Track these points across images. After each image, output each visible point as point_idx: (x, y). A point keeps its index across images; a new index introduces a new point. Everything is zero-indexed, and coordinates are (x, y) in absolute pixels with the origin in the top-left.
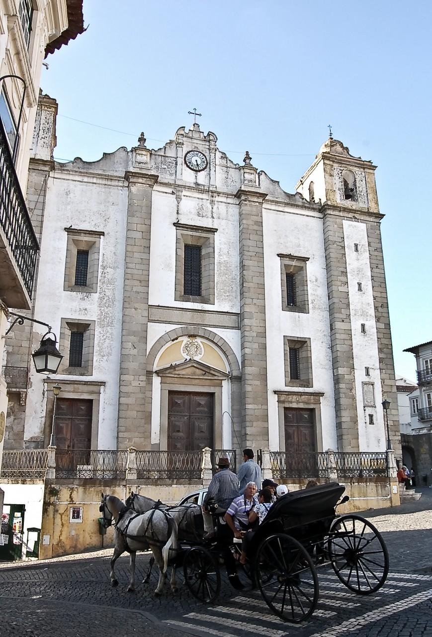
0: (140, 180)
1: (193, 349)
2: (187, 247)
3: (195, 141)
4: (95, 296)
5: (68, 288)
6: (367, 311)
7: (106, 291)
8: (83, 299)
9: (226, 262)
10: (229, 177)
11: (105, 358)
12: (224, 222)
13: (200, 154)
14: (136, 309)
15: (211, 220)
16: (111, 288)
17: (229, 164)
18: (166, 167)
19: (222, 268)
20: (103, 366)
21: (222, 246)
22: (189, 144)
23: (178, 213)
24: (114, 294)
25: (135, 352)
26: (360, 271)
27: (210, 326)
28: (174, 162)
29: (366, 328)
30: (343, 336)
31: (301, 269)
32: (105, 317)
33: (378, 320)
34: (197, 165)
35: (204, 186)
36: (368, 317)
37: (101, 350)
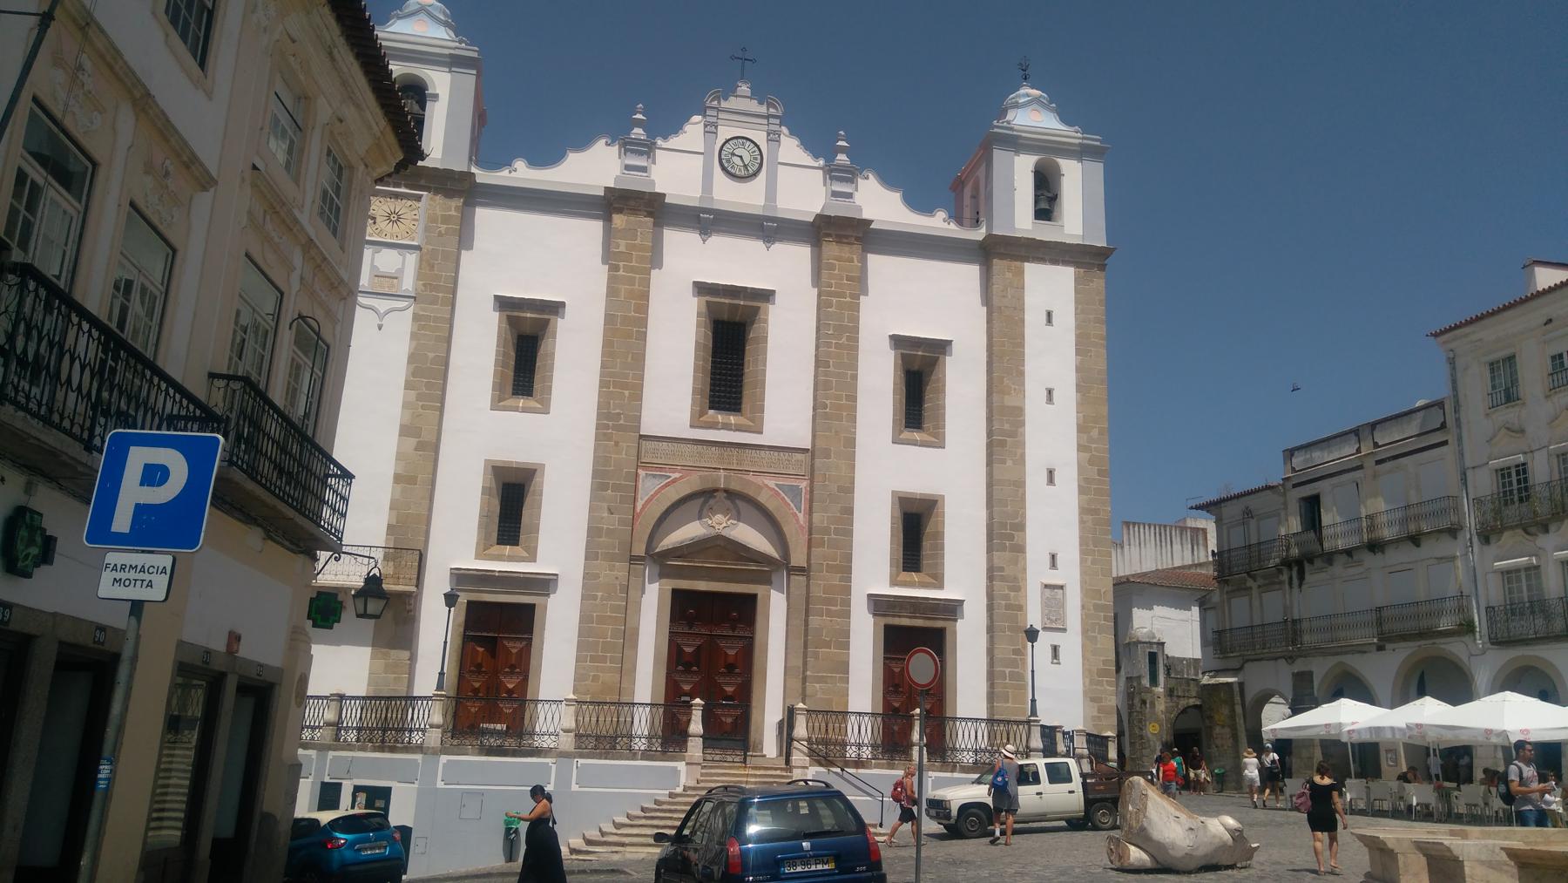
5: (498, 403)
20: (560, 543)
34: (745, 166)
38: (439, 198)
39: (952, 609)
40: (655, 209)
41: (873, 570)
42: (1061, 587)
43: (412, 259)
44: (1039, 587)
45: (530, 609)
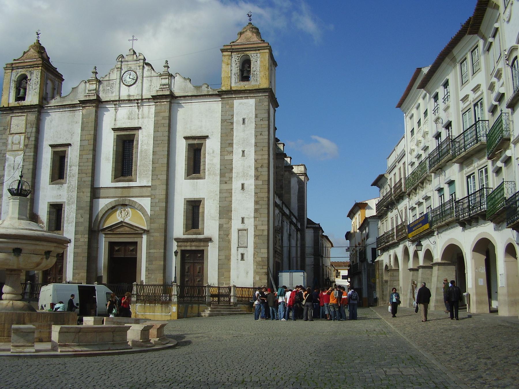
1: (123, 213)
2: (124, 142)
3: (129, 63)
4: (65, 186)
8: (59, 189)
10: (152, 84)
14: (83, 192)
15: (137, 120)
23: (115, 120)
25: (81, 220)
27: (133, 197)
29: (245, 186)
30: (225, 195)
31: (201, 144)
32: (71, 199)
33: (257, 178)
35: (133, 96)
37: (68, 220)
38: (30, 115)
39: (209, 240)
41: (178, 229)
43: (23, 137)
44: (237, 231)
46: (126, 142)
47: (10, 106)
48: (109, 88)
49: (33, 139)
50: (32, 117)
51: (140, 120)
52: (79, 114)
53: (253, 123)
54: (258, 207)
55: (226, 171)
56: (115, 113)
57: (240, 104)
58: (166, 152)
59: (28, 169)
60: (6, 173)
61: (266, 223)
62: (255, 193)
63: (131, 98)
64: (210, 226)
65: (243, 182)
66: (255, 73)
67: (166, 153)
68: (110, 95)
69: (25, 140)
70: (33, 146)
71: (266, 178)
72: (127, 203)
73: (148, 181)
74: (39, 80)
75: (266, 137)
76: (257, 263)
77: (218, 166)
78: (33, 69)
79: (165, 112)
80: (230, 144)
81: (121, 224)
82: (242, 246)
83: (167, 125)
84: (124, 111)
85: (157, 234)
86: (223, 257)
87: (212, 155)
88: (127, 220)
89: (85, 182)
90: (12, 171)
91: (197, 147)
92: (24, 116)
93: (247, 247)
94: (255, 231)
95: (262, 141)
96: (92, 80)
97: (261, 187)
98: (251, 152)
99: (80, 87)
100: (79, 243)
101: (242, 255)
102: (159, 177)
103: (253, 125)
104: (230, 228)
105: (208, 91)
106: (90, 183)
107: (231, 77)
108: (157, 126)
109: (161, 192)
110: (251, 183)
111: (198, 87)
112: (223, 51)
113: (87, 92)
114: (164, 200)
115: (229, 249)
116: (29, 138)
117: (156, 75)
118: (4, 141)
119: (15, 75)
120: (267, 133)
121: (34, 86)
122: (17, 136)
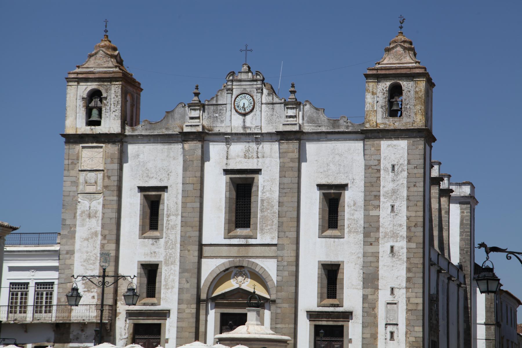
0: (192, 137)
4: (162, 241)
6: (398, 232)
7: (170, 235)
8: (153, 244)
9: (268, 199)
10: (275, 113)
11: (170, 290)
12: (268, 161)
13: (247, 96)
15: (255, 160)
16: (173, 232)
17: (276, 100)
18: (217, 115)
19: (264, 204)
21: (266, 184)
22: (238, 87)
23: (227, 158)
24: (176, 238)
26: (394, 192)
28: (225, 109)
29: (395, 249)
30: (370, 259)
33: (409, 239)
35: (250, 128)
36: (398, 238)
37: (166, 285)
38: (110, 146)
40: (203, 137)
41: (309, 297)
42: (396, 304)
45: (159, 325)
46: (242, 187)
47: (79, 132)
48: (217, 115)
49: (116, 178)
50: (113, 149)
51: (260, 160)
52: (177, 148)
53: (404, 171)
54: (410, 275)
55: (371, 231)
56: (226, 149)
57: (388, 146)
58: (296, 204)
59: (111, 219)
60: (78, 223)
61: (421, 295)
62: (408, 258)
63: (248, 131)
64: (351, 297)
65: (392, 244)
66: (408, 106)
67: (296, 204)
68: (219, 124)
69: (104, 179)
70: (115, 188)
71: (421, 241)
72: (245, 264)
73: (273, 238)
74: (120, 100)
75: (422, 189)
76: (410, 343)
77: (362, 222)
78: (109, 83)
79: (293, 152)
80: (375, 196)
81: (239, 292)
82: (391, 322)
83: (297, 169)
84: (237, 148)
85: (286, 305)
86: (368, 336)
87: (353, 207)
88: (245, 287)
89: (190, 237)
90: (88, 220)
91: (333, 196)
92: (101, 147)
93: (397, 325)
94: (407, 305)
95: (416, 194)
96: (194, 105)
97: (414, 251)
98: (402, 206)
99: (177, 110)
100: (184, 315)
101: (392, 333)
102: (287, 234)
103: (405, 174)
104: (377, 300)
105: (347, 127)
106: (197, 239)
107: (376, 111)
108: (283, 170)
109: (288, 254)
110: (401, 245)
111: (335, 122)
112: (367, 76)
113: (187, 118)
114: (294, 263)
115: (376, 325)
116: (109, 177)
117: (280, 101)
118: (74, 179)
119: (85, 89)
120: (422, 183)
121: (112, 106)
122: (93, 174)
